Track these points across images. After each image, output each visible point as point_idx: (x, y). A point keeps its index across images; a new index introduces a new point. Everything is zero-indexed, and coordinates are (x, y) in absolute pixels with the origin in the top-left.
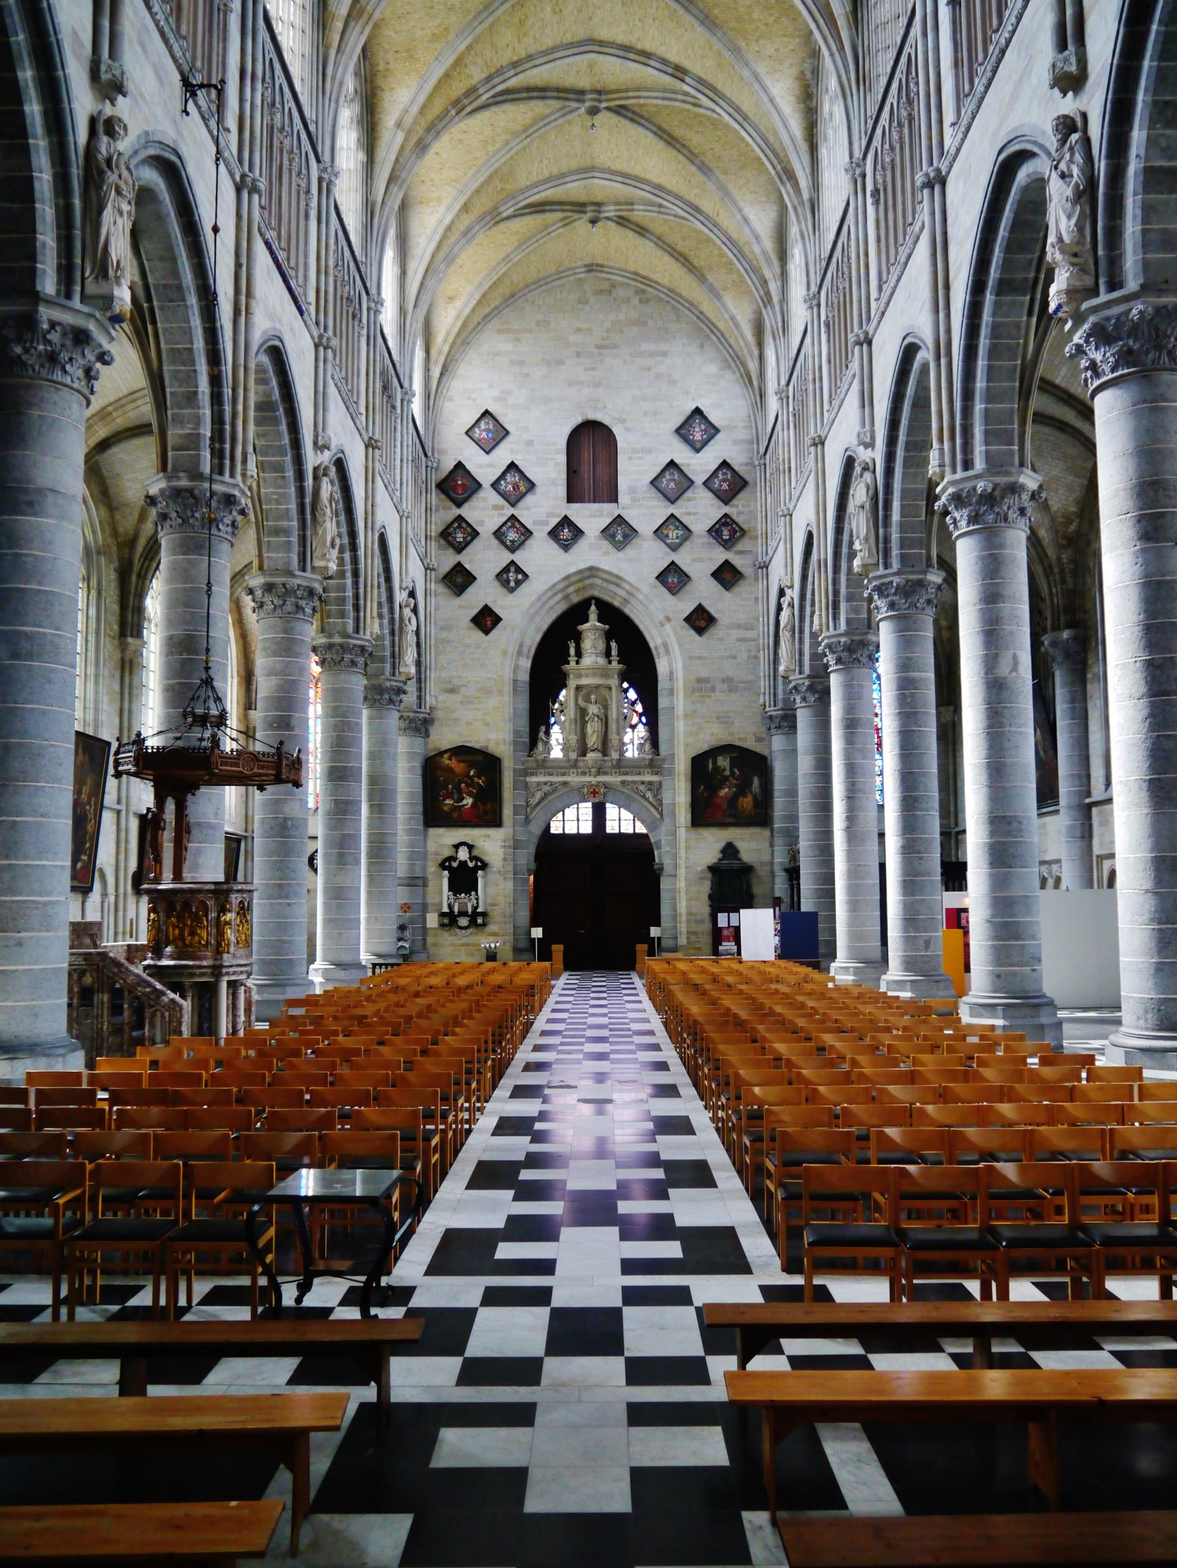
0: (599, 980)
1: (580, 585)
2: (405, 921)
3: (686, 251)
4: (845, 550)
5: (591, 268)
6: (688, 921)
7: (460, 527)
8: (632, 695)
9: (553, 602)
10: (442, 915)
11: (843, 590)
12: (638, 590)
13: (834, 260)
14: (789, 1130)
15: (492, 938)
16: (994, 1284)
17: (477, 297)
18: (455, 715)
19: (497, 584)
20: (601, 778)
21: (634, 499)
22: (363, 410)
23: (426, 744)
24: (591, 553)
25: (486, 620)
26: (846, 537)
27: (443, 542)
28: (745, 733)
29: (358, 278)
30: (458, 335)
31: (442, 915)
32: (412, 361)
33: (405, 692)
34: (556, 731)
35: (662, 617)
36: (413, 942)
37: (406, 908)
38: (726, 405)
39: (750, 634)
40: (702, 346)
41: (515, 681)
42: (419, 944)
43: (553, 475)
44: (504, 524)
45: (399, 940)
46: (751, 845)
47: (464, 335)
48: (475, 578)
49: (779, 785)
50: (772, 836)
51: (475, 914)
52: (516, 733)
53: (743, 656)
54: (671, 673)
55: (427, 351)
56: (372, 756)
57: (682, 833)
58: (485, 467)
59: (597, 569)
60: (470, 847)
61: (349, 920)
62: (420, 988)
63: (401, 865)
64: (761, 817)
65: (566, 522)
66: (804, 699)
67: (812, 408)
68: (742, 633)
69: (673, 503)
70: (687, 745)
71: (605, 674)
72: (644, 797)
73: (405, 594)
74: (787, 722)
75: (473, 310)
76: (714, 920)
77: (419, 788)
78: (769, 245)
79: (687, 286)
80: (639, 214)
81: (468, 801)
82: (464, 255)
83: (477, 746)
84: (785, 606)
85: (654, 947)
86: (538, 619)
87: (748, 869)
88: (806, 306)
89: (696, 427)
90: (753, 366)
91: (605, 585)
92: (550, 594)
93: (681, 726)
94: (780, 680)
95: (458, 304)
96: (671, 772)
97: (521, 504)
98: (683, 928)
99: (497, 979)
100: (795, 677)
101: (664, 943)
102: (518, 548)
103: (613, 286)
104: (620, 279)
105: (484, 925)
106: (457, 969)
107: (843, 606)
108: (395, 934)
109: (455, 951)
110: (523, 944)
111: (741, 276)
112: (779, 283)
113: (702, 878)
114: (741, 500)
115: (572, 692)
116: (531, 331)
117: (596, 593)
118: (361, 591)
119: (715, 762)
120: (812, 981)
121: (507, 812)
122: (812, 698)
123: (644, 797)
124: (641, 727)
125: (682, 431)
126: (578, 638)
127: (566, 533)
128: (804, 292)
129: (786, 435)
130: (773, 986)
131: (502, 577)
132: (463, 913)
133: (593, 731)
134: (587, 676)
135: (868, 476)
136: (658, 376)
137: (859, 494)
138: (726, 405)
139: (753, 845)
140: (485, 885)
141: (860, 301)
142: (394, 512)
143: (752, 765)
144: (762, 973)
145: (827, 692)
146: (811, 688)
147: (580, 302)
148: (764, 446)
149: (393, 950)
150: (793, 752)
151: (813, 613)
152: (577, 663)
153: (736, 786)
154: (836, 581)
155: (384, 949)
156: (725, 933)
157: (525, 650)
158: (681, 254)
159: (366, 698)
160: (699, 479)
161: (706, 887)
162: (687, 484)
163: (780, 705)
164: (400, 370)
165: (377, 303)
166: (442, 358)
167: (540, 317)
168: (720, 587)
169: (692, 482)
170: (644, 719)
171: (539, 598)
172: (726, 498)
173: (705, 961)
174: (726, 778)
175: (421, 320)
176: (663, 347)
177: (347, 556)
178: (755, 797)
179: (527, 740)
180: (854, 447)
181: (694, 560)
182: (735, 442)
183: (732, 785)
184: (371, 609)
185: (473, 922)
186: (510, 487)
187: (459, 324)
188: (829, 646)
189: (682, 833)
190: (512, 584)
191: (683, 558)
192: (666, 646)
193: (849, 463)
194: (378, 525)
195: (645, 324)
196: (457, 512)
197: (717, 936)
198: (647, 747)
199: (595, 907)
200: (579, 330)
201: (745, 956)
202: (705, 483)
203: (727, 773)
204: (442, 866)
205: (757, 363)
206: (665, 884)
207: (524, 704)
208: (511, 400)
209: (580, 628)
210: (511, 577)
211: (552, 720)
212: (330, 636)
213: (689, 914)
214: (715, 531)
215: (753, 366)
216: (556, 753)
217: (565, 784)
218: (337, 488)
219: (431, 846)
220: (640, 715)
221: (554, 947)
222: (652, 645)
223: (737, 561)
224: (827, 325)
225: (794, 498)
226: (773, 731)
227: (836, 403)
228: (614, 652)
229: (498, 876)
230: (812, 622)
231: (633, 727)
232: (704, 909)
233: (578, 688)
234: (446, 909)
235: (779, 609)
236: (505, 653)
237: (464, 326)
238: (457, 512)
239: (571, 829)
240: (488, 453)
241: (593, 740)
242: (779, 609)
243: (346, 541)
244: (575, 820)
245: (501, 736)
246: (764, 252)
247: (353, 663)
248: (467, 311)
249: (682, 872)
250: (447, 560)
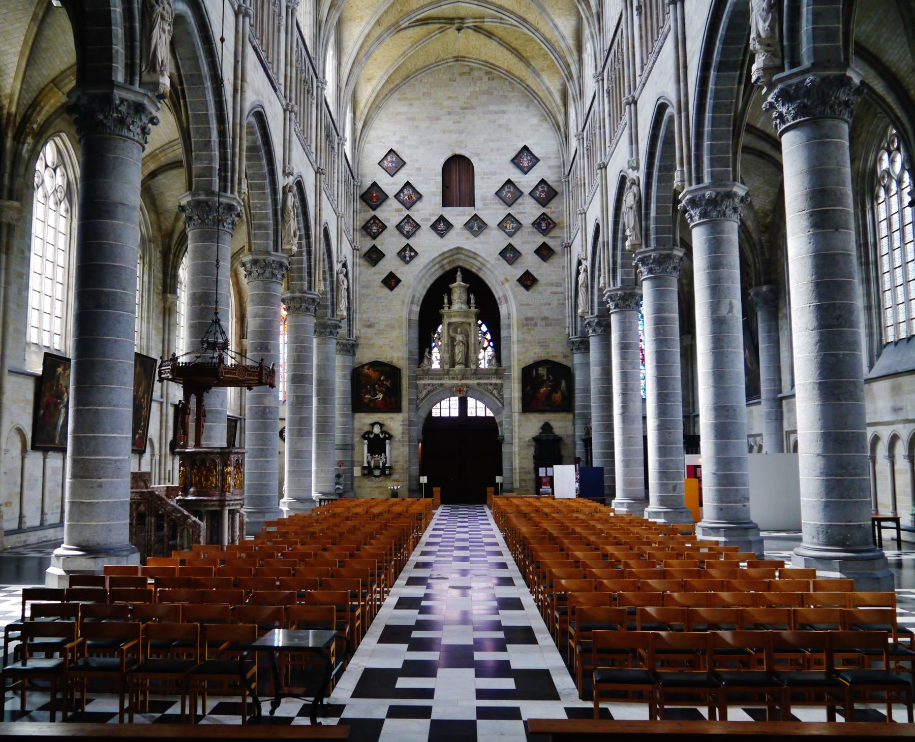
0: (463, 510)
1: (451, 259)
2: (340, 472)
3: (518, 47)
4: (620, 235)
5: (457, 59)
6: (520, 473)
7: (374, 223)
8: (484, 328)
9: (433, 270)
10: (364, 468)
11: (619, 261)
12: (487, 261)
13: (613, 51)
14: (584, 608)
15: (395, 483)
16: (717, 709)
17: (386, 78)
18: (372, 342)
19: (398, 258)
20: (464, 382)
21: (485, 204)
22: (314, 150)
23: (353, 360)
24: (458, 238)
25: (391, 281)
26: (621, 227)
27: (364, 232)
28: (556, 352)
29: (311, 68)
30: (374, 102)
31: (364, 468)
32: (344, 119)
33: (340, 327)
34: (435, 350)
35: (503, 279)
36: (345, 485)
37: (341, 463)
38: (543, 143)
40: (528, 107)
41: (410, 320)
42: (349, 486)
43: (434, 190)
44: (403, 220)
45: (336, 484)
46: (560, 424)
47: (377, 102)
48: (384, 255)
49: (578, 386)
50: (574, 418)
51: (384, 468)
52: (411, 353)
53: (555, 303)
54: (509, 315)
55: (354, 113)
56: (319, 367)
57: (516, 416)
58: (390, 185)
59: (462, 249)
60: (381, 425)
61: (304, 471)
62: (350, 515)
63: (337, 436)
64: (567, 405)
65: (442, 219)
66: (594, 331)
67: (598, 145)
68: (555, 289)
69: (510, 206)
70: (519, 360)
71: (466, 315)
72: (491, 393)
73: (340, 265)
74: (583, 346)
75: (383, 87)
76: (537, 472)
77: (349, 389)
78: (571, 42)
79: (518, 69)
80: (488, 25)
81: (380, 396)
82: (377, 52)
83: (385, 361)
84: (582, 271)
85: (498, 489)
86: (424, 281)
87: (558, 440)
88: (594, 80)
89: (524, 158)
90: (561, 119)
91: (466, 258)
92: (431, 265)
93: (515, 348)
94: (579, 319)
95: (374, 83)
96: (509, 377)
97: (414, 208)
98: (517, 477)
99: (398, 509)
100: (588, 317)
101: (505, 487)
102: (411, 236)
103: (471, 70)
104: (476, 65)
105: (390, 475)
106: (374, 503)
107: (619, 271)
108: (334, 480)
109: (372, 491)
110: (415, 487)
111: (553, 61)
112: (577, 66)
113: (528, 445)
114: (553, 204)
115: (446, 327)
116: (419, 99)
117: (461, 264)
118: (313, 264)
119: (537, 371)
120: (600, 512)
121: (405, 403)
122: (599, 330)
123: (491, 393)
124: (489, 349)
126: (449, 292)
127: (442, 226)
128: (594, 71)
129: (582, 163)
130: (574, 515)
131: (401, 254)
133: (459, 350)
134: (455, 316)
135: (635, 188)
136: (500, 126)
137: (629, 200)
138: (543, 143)
139: (561, 424)
140: (391, 450)
141: (629, 77)
142: (333, 214)
144: (567, 506)
145: (608, 327)
146: (598, 324)
147: (450, 80)
148: (568, 170)
149: (333, 491)
150: (587, 365)
151: (599, 276)
152: (449, 308)
153: (551, 386)
154: (614, 256)
155: (326, 490)
156: (544, 480)
157: (416, 300)
158: (515, 49)
159: (315, 331)
160: (526, 191)
161: (531, 451)
162: (519, 194)
163: (579, 334)
164: (337, 125)
165: (322, 83)
166: (364, 117)
167: (425, 90)
168: (540, 260)
169: (522, 193)
170: (491, 344)
171: (425, 267)
172: (544, 203)
173: (531, 498)
174: (545, 381)
175: (350, 93)
176: (503, 107)
177: (304, 242)
178: (563, 393)
179: (417, 357)
180: (625, 170)
181: (523, 243)
182: (550, 167)
183: (549, 386)
184: (319, 275)
185: (383, 473)
186: (406, 197)
187: (374, 95)
188: (610, 297)
189: (516, 416)
190: (408, 258)
191: (516, 242)
192: (505, 297)
193: (623, 180)
194: (323, 222)
195: (492, 93)
196: (372, 213)
197: (539, 482)
198: (494, 361)
199: (461, 464)
200: (450, 98)
201: (557, 495)
202: (530, 194)
203: (545, 378)
205: (563, 116)
206: (505, 449)
207: (415, 334)
208: (407, 142)
209: (451, 286)
210: (407, 254)
211: (433, 344)
212: (293, 292)
213: (521, 468)
214: (537, 224)
215: (561, 119)
216: (436, 365)
217: (441, 385)
218: (297, 199)
219: (357, 425)
220: (489, 341)
221: (435, 489)
222: (496, 296)
223: (551, 243)
224: (608, 92)
225: (588, 203)
226: (574, 351)
227: (614, 142)
228: (472, 301)
229: (398, 444)
230: (599, 282)
231: (485, 349)
232: (531, 465)
233: (450, 324)
234: (366, 465)
235: (578, 273)
236: (403, 302)
237: (377, 96)
238: (372, 213)
239: (445, 414)
240: (392, 176)
241: (459, 357)
242: (578, 273)
243: (303, 232)
244: (448, 408)
245: (400, 354)
246: (568, 47)
247: (308, 309)
248: (379, 87)
249: (516, 441)
250: (366, 244)
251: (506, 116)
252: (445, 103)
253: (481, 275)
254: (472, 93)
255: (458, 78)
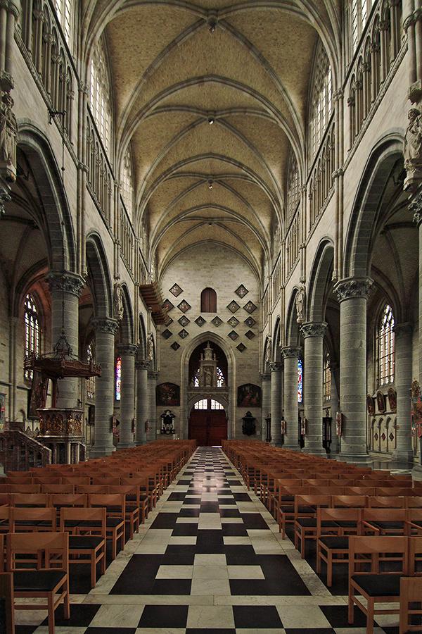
10: (162, 430)
25: (175, 346)
31: (162, 430)
38: (251, 284)
39: (257, 352)
40: (244, 266)
49: (264, 395)
58: (176, 301)
60: (170, 411)
65: (200, 318)
71: (213, 362)
73: (149, 336)
74: (268, 377)
80: (225, 222)
81: (170, 398)
89: (241, 291)
97: (187, 312)
114: (254, 313)
121: (181, 402)
125: (237, 292)
126: (204, 352)
127: (200, 321)
132: (168, 430)
135: (303, 292)
136: (230, 274)
137: (300, 298)
143: (257, 390)
148: (263, 296)
150: (269, 387)
160: (242, 307)
176: (232, 266)
181: (240, 330)
182: (254, 295)
183: (250, 395)
191: (236, 330)
199: (206, 430)
200: (205, 260)
204: (161, 416)
210: (183, 334)
214: (246, 322)
216: (197, 385)
233: (204, 367)
239: (201, 408)
241: (208, 382)
244: (201, 405)
251: (233, 270)
252: (203, 263)
253: (219, 345)
254: (217, 258)
255: (209, 250)
